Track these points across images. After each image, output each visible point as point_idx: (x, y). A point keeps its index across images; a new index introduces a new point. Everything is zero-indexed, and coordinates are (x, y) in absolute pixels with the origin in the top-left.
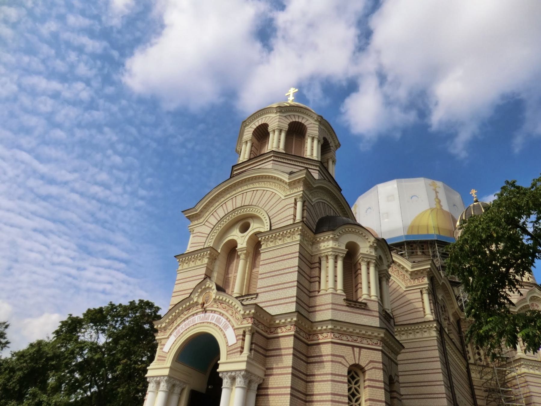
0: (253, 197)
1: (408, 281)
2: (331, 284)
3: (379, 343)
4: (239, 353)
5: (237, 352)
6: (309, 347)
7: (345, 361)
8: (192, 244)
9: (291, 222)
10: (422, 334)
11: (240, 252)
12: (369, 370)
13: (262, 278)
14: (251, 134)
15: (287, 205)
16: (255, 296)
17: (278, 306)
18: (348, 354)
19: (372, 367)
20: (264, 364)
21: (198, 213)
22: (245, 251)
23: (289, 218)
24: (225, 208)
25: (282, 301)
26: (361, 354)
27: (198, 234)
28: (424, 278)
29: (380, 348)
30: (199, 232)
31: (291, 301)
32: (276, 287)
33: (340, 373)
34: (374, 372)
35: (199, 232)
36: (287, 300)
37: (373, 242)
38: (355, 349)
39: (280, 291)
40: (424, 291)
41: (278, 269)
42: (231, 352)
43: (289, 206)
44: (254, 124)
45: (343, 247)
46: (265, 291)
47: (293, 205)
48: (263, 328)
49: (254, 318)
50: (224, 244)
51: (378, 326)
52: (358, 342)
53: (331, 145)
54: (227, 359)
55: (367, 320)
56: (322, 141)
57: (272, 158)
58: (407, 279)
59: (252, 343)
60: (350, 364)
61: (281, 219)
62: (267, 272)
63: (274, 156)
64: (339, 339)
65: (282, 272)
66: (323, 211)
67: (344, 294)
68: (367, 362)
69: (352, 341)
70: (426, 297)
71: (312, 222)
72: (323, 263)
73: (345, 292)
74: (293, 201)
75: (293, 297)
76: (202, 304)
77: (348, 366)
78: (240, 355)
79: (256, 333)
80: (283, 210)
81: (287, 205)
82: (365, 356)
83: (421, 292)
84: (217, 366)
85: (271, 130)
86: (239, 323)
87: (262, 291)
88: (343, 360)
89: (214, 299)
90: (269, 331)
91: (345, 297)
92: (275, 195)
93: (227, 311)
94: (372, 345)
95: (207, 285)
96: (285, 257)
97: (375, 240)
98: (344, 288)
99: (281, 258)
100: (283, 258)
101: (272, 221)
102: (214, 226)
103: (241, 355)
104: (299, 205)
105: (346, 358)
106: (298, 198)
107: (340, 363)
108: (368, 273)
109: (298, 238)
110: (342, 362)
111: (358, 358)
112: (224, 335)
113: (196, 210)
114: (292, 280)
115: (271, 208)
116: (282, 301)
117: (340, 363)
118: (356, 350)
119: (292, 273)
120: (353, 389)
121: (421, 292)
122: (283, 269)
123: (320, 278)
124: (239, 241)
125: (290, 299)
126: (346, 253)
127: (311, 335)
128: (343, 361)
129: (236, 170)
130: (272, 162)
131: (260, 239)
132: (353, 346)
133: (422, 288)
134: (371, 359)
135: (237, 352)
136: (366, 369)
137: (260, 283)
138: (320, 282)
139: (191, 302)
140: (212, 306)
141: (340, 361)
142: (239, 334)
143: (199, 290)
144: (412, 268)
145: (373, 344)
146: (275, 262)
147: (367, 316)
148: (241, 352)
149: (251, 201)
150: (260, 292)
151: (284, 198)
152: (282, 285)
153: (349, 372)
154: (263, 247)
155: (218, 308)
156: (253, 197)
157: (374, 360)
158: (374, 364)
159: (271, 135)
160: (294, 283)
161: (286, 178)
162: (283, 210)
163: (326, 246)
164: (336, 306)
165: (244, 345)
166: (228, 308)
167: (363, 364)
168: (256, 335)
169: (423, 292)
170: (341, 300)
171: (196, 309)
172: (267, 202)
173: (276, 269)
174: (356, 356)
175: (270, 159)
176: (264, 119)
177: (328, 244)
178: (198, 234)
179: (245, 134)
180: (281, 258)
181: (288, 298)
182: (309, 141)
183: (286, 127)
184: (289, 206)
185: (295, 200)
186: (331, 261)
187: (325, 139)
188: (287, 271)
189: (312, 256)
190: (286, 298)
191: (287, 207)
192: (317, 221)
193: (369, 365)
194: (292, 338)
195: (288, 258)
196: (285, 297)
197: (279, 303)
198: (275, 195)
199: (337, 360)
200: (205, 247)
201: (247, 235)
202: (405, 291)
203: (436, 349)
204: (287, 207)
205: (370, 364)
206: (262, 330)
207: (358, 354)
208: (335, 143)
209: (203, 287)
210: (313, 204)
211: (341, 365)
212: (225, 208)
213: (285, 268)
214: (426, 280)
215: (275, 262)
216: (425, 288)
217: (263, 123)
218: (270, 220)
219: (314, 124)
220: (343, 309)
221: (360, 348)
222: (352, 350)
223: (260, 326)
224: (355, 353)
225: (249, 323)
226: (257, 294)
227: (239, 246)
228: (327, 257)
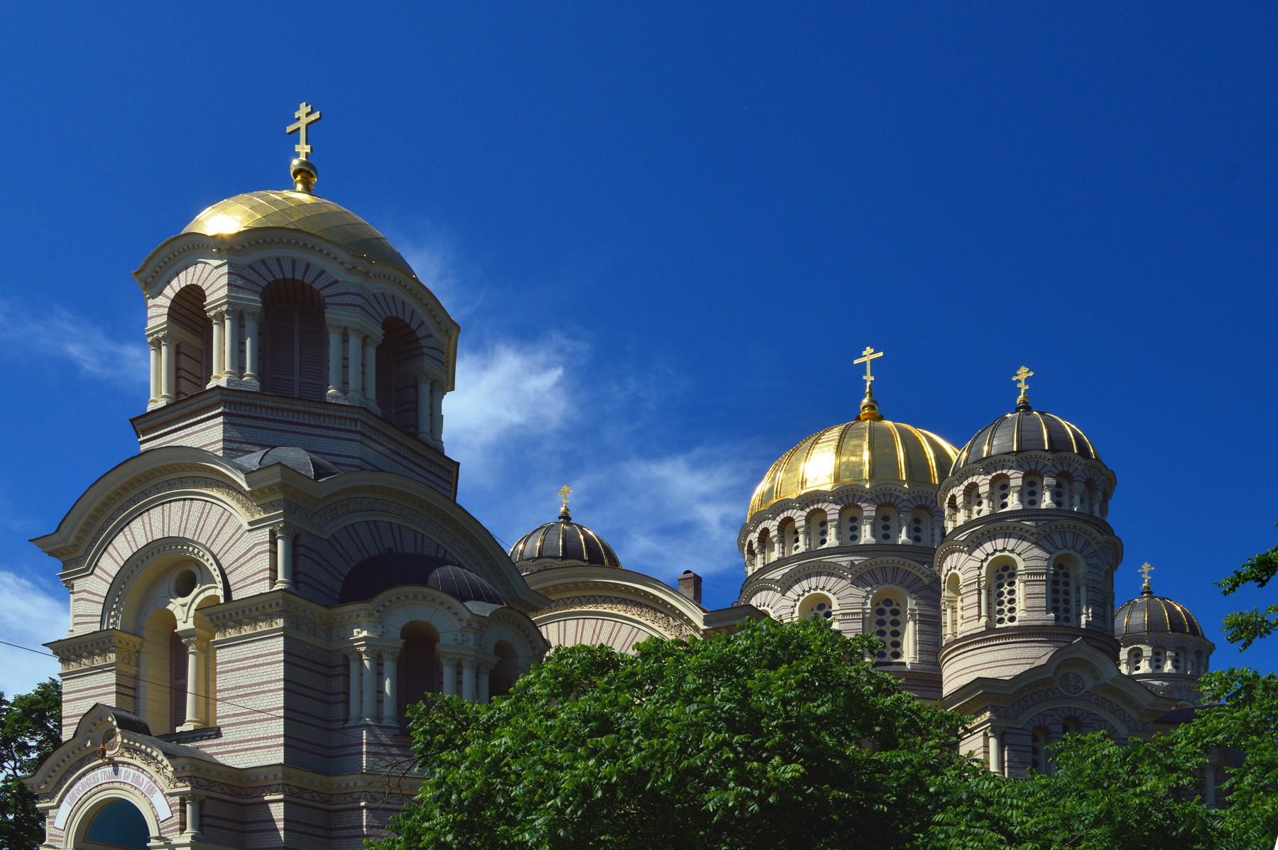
17: (255, 751)
25: (262, 743)
27: (85, 595)
36: (270, 742)
39: (257, 725)
41: (249, 683)
46: (230, 722)
62: (230, 686)
65: (257, 689)
87: (226, 723)
96: (261, 660)
99: (253, 662)
116: (262, 743)
122: (259, 684)
146: (243, 668)
150: (222, 724)
160: (279, 711)
173: (246, 683)
178: (85, 595)
180: (253, 662)
181: (271, 738)
188: (265, 688)
196: (265, 735)
197: (256, 746)
213: (261, 681)
215: (243, 668)
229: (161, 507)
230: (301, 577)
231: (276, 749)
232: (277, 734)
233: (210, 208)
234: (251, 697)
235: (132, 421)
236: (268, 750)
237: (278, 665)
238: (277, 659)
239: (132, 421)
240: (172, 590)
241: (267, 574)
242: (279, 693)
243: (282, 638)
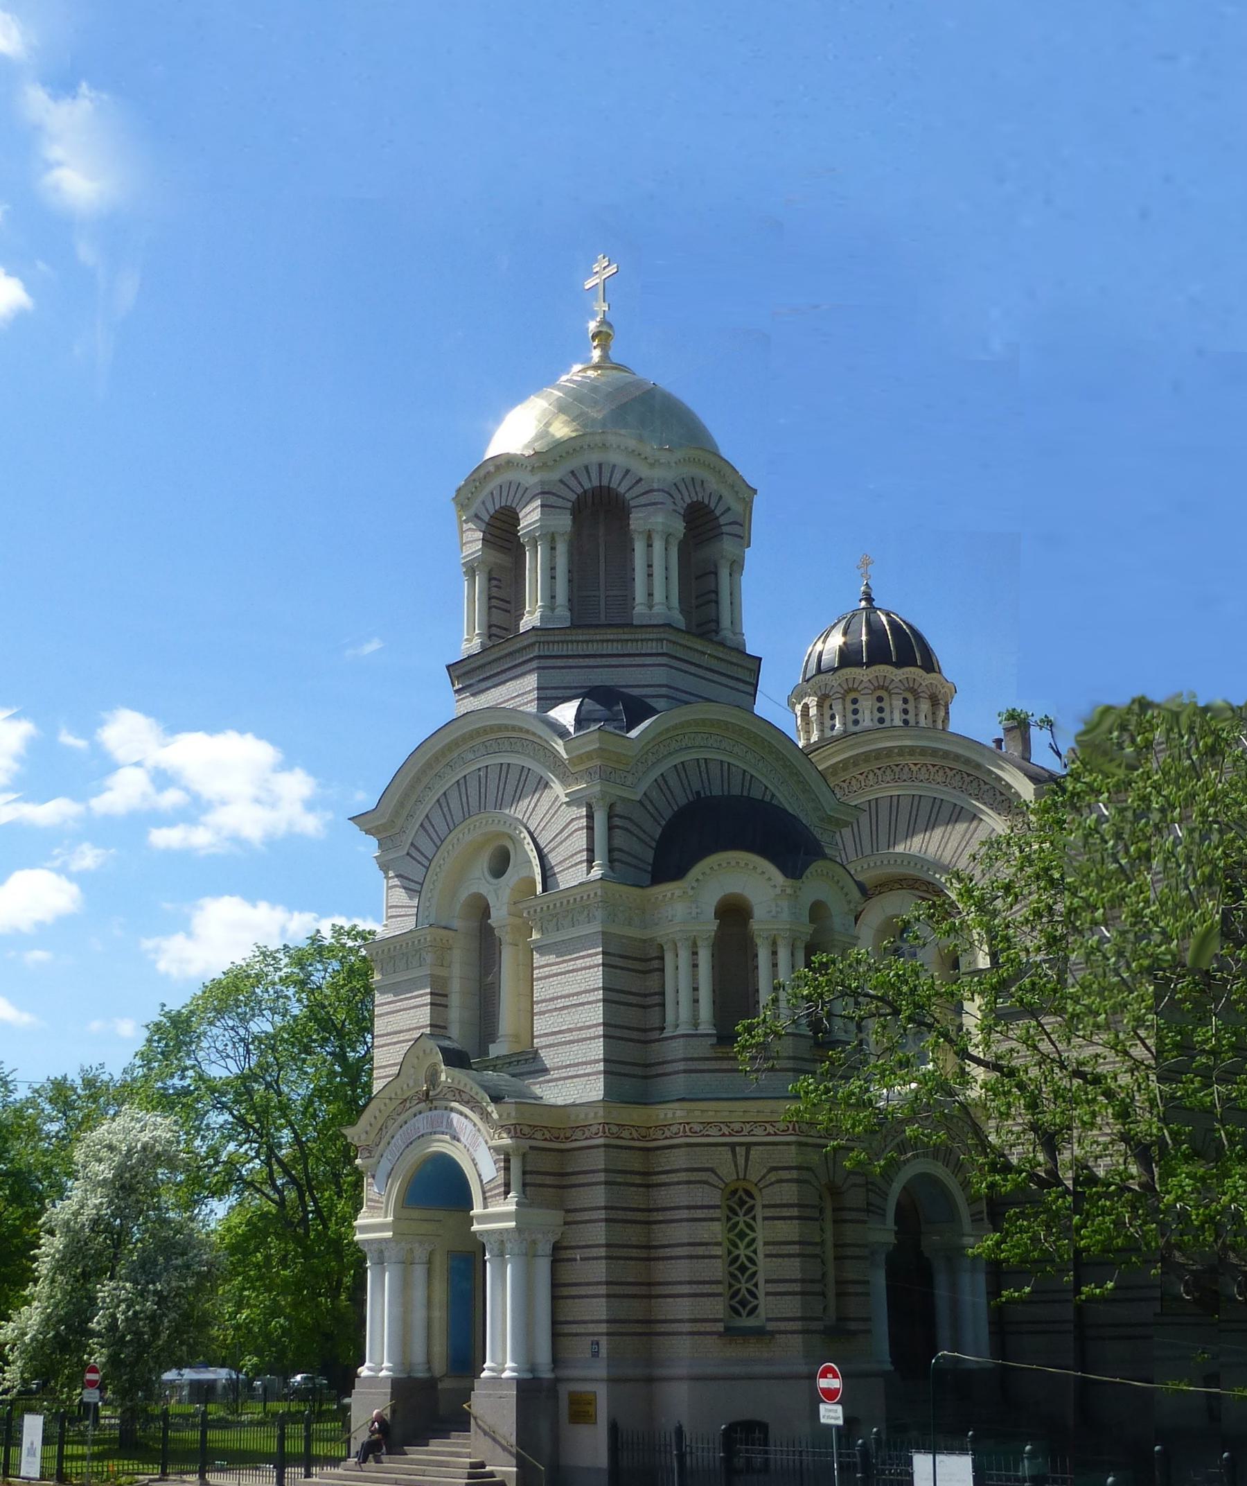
2: (684, 1012)
3: (791, 1128)
5: (498, 1195)
7: (716, 1178)
17: (575, 1080)
19: (773, 1179)
20: (560, 1205)
32: (568, 1036)
39: (575, 1047)
56: (679, 527)
59: (524, 1173)
64: (703, 1136)
69: (731, 1135)
72: (669, 957)
75: (597, 1061)
78: (506, 1198)
84: (470, 1221)
88: (713, 1176)
108: (775, 965)
110: (711, 1181)
112: (473, 1160)
120: (742, 1225)
122: (577, 994)
123: (663, 994)
128: (712, 1178)
130: (534, 664)
132: (732, 1146)
134: (775, 1165)
135: (498, 1195)
141: (704, 1179)
150: (540, 1045)
165: (509, 1179)
182: (639, 547)
186: (684, 955)
189: (645, 941)
221: (749, 1146)
223: (538, 1135)
230: (616, 855)
231: (595, 1077)
232: (597, 1057)
233: (519, 407)
235: (448, 667)
237: (596, 969)
238: (596, 962)
239: (448, 667)
240: (486, 873)
241: (584, 856)
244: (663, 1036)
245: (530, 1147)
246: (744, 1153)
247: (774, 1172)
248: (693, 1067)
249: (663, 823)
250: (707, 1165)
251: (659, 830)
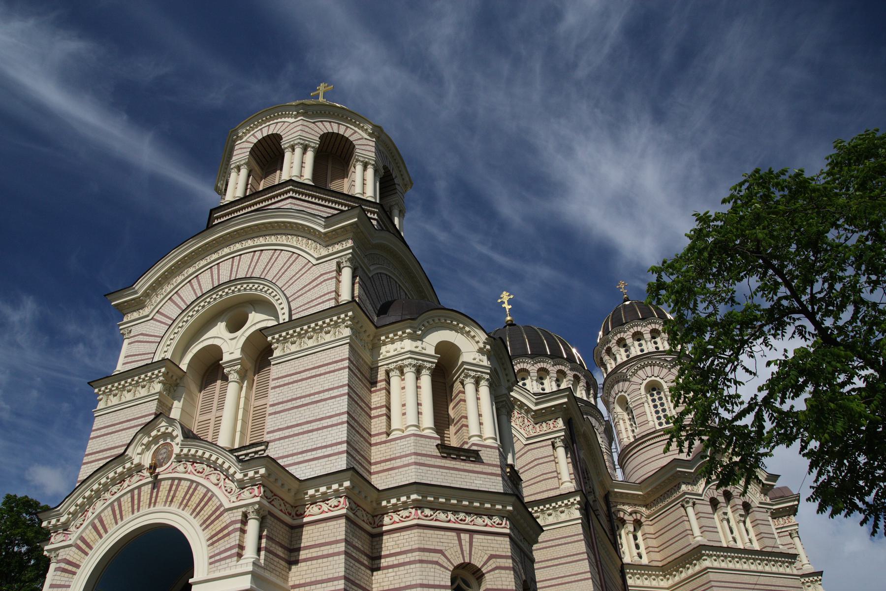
0: (253, 264)
1: (531, 427)
2: (411, 419)
3: (504, 523)
4: (235, 558)
6: (375, 539)
8: (126, 357)
9: (332, 303)
10: (557, 516)
11: (228, 369)
12: (488, 572)
13: (275, 413)
14: (248, 153)
15: (321, 275)
16: (263, 447)
17: (311, 463)
18: (452, 545)
19: (494, 566)
21: (139, 297)
22: (239, 366)
23: (327, 297)
24: (196, 286)
25: (320, 453)
26: (474, 544)
27: (141, 338)
28: (557, 421)
29: (508, 531)
30: (142, 334)
31: (336, 451)
33: (437, 583)
34: (498, 575)
35: (142, 334)
36: (329, 451)
37: (484, 343)
38: (462, 535)
40: (559, 443)
41: (308, 393)
42: (218, 558)
43: (326, 277)
44: (253, 135)
45: (431, 351)
47: (334, 274)
48: (283, 507)
49: (264, 486)
50: (195, 355)
51: (502, 491)
52: (466, 522)
53: (396, 181)
54: (209, 573)
55: (481, 482)
57: (291, 194)
58: (529, 424)
60: (455, 565)
61: (312, 301)
62: (285, 399)
63: (294, 191)
66: (387, 291)
67: (436, 436)
68: (486, 557)
70: (561, 452)
71: (370, 307)
73: (438, 433)
74: (334, 267)
76: (151, 467)
77: (451, 568)
78: (238, 561)
79: (269, 517)
80: (314, 284)
81: (321, 275)
82: (481, 548)
83: (553, 444)
85: (286, 146)
86: (234, 499)
87: (278, 437)
88: (442, 557)
89: (178, 455)
90: (293, 513)
91: (439, 442)
92: (296, 258)
93: (207, 477)
94: (493, 526)
95: (163, 429)
97: (486, 339)
98: (435, 426)
99: (313, 372)
100: (318, 371)
101: (294, 305)
102: (174, 321)
103: (241, 562)
104: (347, 273)
105: (446, 553)
106: (344, 259)
107: (437, 563)
109: (347, 332)
110: (440, 561)
111: (468, 552)
113: (136, 293)
114: (338, 412)
115: (291, 282)
117: (437, 563)
118: (465, 537)
119: (338, 399)
121: (553, 444)
124: (225, 348)
125: (334, 447)
126: (436, 361)
127: (376, 516)
129: (217, 218)
131: (269, 338)
133: (555, 438)
136: (484, 570)
137: (271, 423)
138: (389, 417)
139: (128, 465)
140: (174, 470)
141: (435, 559)
142: (233, 519)
143: (146, 440)
144: (537, 404)
145: (495, 525)
147: (479, 475)
148: (240, 556)
149: (251, 270)
151: (315, 262)
152: (318, 423)
153: (453, 580)
154: (276, 353)
155: (186, 472)
156: (253, 264)
157: (498, 553)
158: (498, 560)
159: (288, 155)
161: (319, 225)
162: (314, 284)
163: (399, 349)
164: (424, 458)
166: (208, 470)
167: (477, 562)
168: (270, 520)
169: (556, 445)
170: (431, 447)
171: (138, 478)
172: (283, 271)
173: (304, 394)
174: (464, 547)
175: (286, 196)
176: (272, 127)
177: (402, 346)
178: (141, 338)
179: (235, 153)
180: (313, 372)
183: (315, 141)
184: (326, 277)
185: (338, 264)
187: (385, 168)
190: (326, 447)
191: (321, 279)
192: (378, 308)
193: (488, 564)
194: (343, 521)
195: (328, 370)
196: (324, 444)
197: (312, 457)
198: (296, 258)
199: (430, 559)
200: (155, 360)
201: (242, 335)
202: (526, 445)
203: (581, 540)
204: (321, 279)
205: (491, 562)
206: (281, 510)
207: (468, 544)
208: (403, 179)
209: (154, 433)
210: (370, 276)
211: (437, 567)
212: (196, 286)
214: (560, 424)
216: (559, 437)
217: (270, 133)
218: (289, 303)
219: (366, 139)
220: (437, 464)
221: (472, 532)
222: (456, 538)
224: (463, 543)
225: (255, 496)
226: (267, 444)
227: (226, 358)
228: (401, 370)
229: (221, 282)
231: (336, 457)
234: (309, 407)
236: (326, 459)
242: (342, 398)
243: (347, 346)
244: (391, 437)
245: (269, 512)
246: (468, 540)
247: (494, 560)
248: (422, 461)
249: (381, 303)
250: (437, 548)
251: (380, 306)
